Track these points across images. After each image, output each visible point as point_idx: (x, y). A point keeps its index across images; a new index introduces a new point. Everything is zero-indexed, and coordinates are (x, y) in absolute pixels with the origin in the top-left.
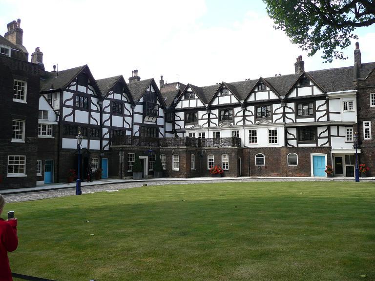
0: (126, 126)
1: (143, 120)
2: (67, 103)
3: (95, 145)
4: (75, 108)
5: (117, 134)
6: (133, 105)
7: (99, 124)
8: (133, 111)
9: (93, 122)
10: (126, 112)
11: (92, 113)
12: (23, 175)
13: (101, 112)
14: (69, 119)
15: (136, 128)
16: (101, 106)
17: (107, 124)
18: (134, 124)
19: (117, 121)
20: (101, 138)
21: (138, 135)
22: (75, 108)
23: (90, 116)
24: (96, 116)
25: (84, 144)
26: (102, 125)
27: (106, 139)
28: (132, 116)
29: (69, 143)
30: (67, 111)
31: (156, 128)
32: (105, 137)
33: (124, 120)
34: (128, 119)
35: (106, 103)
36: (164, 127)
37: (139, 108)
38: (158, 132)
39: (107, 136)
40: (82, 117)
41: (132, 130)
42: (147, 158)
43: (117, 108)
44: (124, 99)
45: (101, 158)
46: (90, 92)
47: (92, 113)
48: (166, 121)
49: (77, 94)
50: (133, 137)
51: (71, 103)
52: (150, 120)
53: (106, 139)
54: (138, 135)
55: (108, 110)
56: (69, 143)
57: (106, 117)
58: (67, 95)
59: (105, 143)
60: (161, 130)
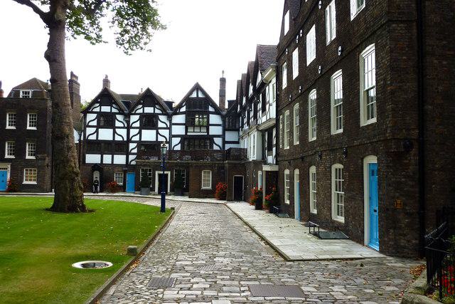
0: (161, 139)
1: (186, 131)
2: (90, 124)
3: (120, 159)
4: (98, 127)
5: (149, 149)
6: (170, 118)
7: (125, 139)
8: (170, 121)
9: (118, 138)
10: (160, 125)
11: (117, 130)
12: (35, 183)
13: (129, 128)
14: (93, 137)
15: (176, 141)
16: (128, 122)
17: (137, 138)
18: (172, 136)
19: (149, 135)
20: (128, 153)
21: (178, 148)
22: (98, 127)
23: (115, 132)
24: (123, 132)
25: (107, 159)
26: (129, 140)
27: (134, 154)
28: (170, 129)
29: (92, 159)
30: (89, 131)
31: (210, 138)
32: (133, 151)
33: (158, 133)
34: (166, 133)
35: (134, 118)
36: (223, 136)
37: (180, 119)
38: (212, 142)
39: (135, 151)
40: (106, 134)
41: (170, 143)
42: (169, 173)
43: (148, 122)
44: (157, 111)
45: (125, 172)
46: (114, 110)
47: (117, 130)
48: (224, 130)
49: (100, 114)
50: (171, 152)
51: (95, 123)
52: (197, 130)
53: (134, 154)
54: (178, 148)
55: (137, 124)
56: (92, 159)
57: (133, 132)
58: (91, 117)
59: (131, 157)
60: (218, 141)
